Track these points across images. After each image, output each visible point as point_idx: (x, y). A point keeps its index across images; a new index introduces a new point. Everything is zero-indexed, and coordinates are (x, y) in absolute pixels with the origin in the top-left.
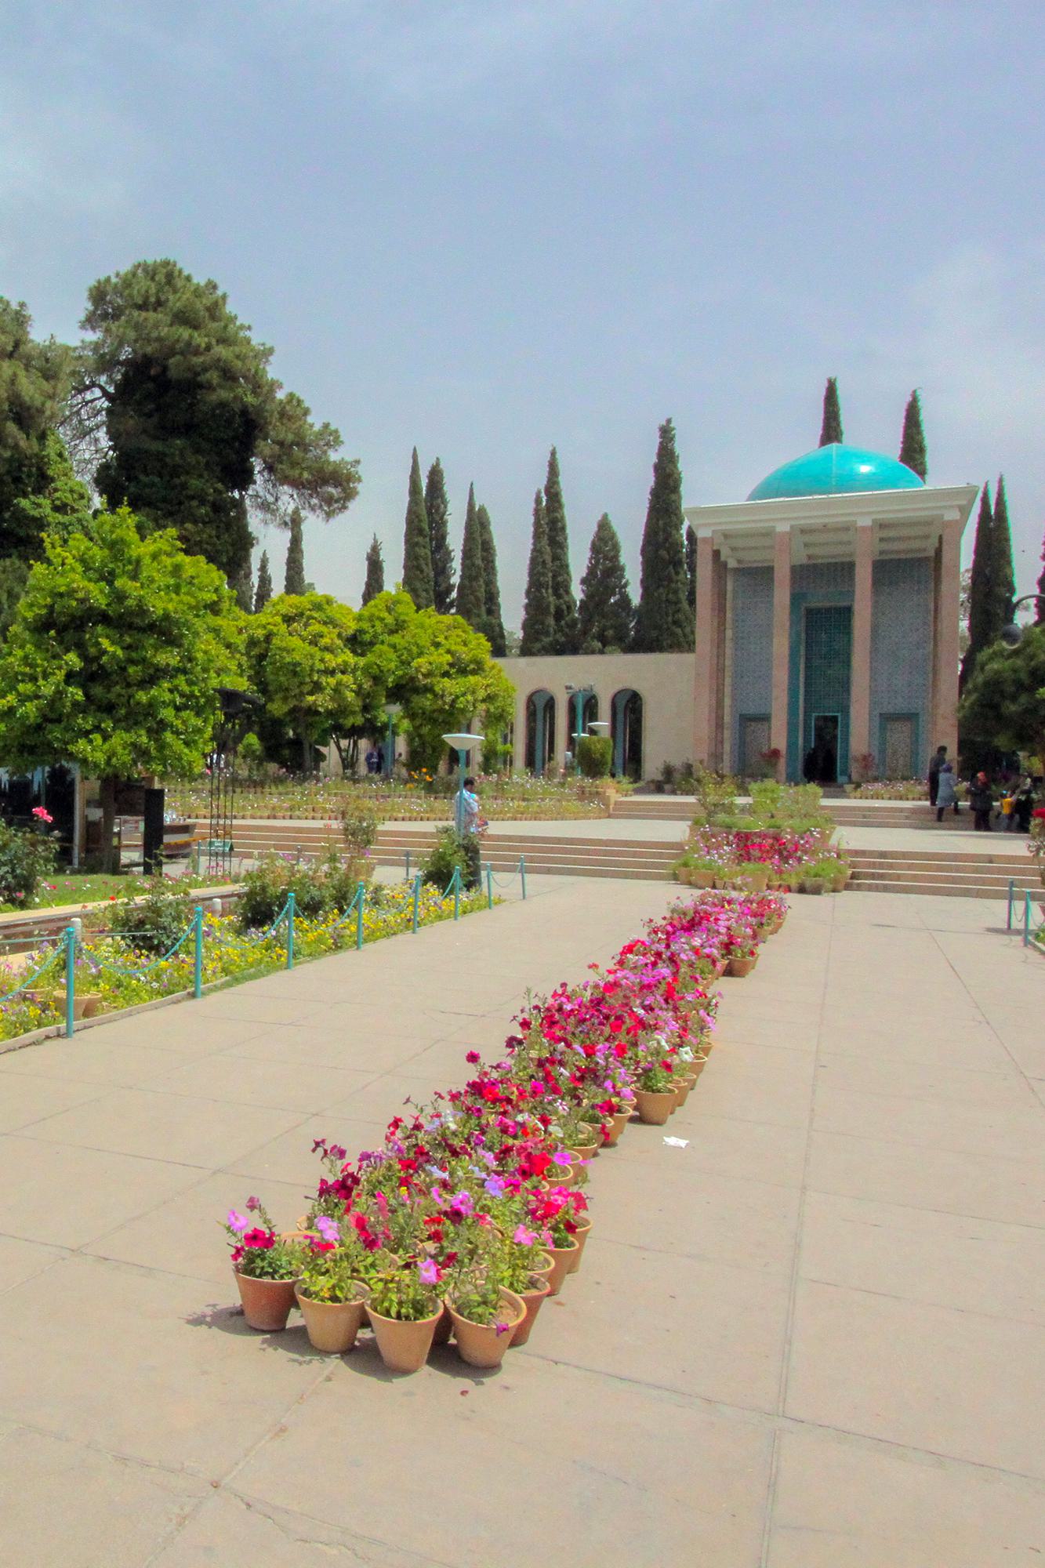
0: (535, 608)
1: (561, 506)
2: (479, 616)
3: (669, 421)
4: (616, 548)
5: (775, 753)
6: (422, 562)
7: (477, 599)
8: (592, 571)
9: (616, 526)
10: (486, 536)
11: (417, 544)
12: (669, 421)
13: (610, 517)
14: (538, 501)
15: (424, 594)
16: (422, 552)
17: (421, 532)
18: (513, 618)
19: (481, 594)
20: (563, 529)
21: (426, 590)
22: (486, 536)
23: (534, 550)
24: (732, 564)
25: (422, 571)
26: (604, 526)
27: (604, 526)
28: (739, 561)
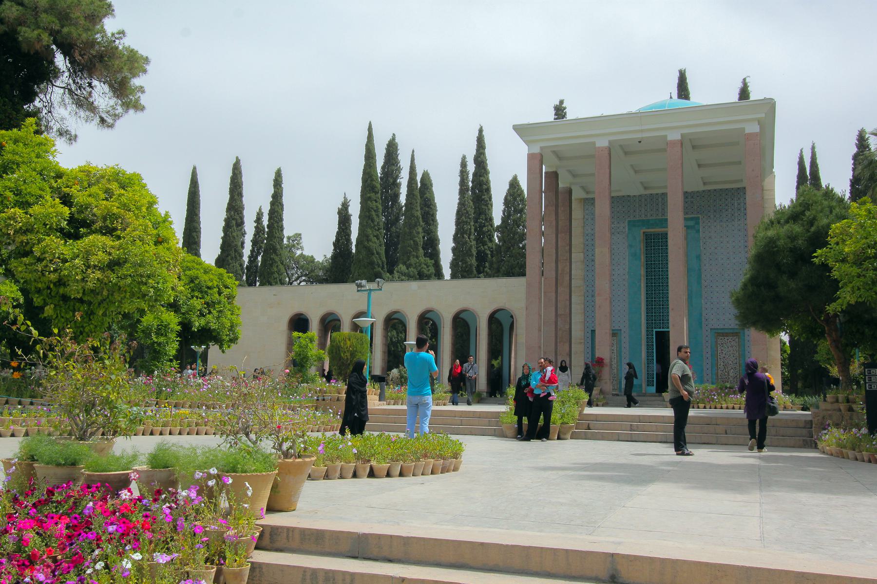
0: (459, 251)
1: (486, 172)
2: (417, 257)
3: (561, 102)
6: (373, 213)
10: (427, 195)
11: (370, 198)
12: (561, 102)
14: (464, 165)
15: (375, 239)
16: (374, 205)
18: (446, 256)
19: (420, 239)
20: (488, 190)
21: (377, 237)
22: (427, 195)
23: (459, 204)
24: (577, 194)
25: (373, 221)
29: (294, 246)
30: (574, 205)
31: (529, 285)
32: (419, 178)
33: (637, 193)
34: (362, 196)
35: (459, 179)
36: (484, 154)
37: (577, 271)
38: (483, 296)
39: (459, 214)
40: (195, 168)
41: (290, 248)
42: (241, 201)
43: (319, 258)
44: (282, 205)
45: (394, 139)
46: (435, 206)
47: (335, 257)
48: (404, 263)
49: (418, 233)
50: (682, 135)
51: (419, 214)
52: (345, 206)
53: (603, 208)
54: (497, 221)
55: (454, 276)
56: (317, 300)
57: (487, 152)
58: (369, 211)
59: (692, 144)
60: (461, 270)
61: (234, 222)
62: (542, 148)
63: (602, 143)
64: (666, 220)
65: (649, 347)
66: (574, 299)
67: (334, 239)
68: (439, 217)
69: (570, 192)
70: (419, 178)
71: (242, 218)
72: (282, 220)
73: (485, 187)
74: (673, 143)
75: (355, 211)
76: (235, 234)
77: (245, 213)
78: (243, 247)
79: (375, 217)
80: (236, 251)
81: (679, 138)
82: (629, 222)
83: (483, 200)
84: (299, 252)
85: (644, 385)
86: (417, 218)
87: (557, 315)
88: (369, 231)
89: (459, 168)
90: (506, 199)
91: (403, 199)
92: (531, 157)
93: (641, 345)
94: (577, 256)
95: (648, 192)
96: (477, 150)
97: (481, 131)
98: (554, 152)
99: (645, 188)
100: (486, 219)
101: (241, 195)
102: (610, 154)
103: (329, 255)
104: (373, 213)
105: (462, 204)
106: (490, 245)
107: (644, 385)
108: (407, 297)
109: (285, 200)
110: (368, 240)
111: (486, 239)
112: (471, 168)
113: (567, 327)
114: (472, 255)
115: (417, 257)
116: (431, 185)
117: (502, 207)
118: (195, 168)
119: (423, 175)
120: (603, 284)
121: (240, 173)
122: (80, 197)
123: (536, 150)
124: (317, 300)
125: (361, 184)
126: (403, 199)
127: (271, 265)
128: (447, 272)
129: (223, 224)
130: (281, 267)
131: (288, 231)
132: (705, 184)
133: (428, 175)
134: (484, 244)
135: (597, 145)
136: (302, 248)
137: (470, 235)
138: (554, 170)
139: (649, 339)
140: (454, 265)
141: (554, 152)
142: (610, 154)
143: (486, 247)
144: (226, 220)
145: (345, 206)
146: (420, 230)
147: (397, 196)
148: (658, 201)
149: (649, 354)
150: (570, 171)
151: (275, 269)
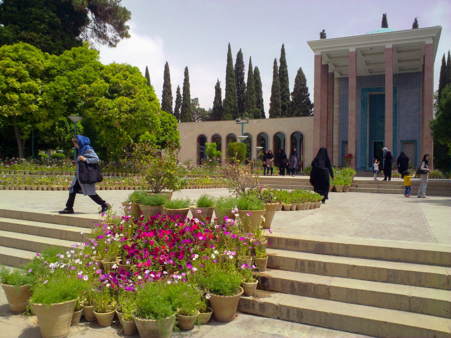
1: (286, 66)
2: (253, 108)
3: (324, 31)
4: (305, 80)
5: (350, 156)
6: (232, 88)
7: (253, 102)
8: (295, 89)
9: (305, 72)
10: (257, 78)
11: (230, 80)
12: (324, 31)
13: (302, 69)
14: (275, 63)
15: (233, 100)
17: (231, 76)
19: (255, 100)
20: (287, 75)
21: (234, 99)
22: (257, 78)
23: (273, 82)
24: (337, 75)
25: (232, 91)
26: (300, 72)
27: (300, 72)
28: (340, 73)
29: (195, 104)
30: (335, 81)
31: (315, 120)
32: (253, 70)
33: (366, 75)
34: (226, 79)
35: (273, 70)
36: (285, 57)
37: (336, 113)
38: (287, 126)
39: (273, 87)
40: (147, 67)
41: (193, 105)
42: (170, 83)
43: (207, 109)
44: (189, 85)
45: (240, 51)
46: (261, 84)
47: (214, 108)
48: (247, 111)
49: (254, 97)
50: (393, 45)
51: (254, 87)
52: (218, 84)
53: (352, 83)
54: (291, 90)
55: (271, 117)
56: (210, 129)
57: (286, 56)
58: (230, 86)
59: (397, 50)
60: (273, 114)
61: (167, 93)
62: (322, 53)
63: (352, 50)
64: (384, 88)
65: (370, 149)
66: (335, 127)
67: (214, 100)
68: (263, 89)
69: (333, 74)
70: (253, 70)
71: (170, 91)
72: (189, 91)
73: (285, 74)
74: (388, 49)
75: (223, 87)
76: (168, 98)
77: (172, 88)
78: (172, 105)
79: (233, 89)
80: (169, 106)
81: (392, 47)
82: (362, 90)
83: (284, 80)
84: (197, 107)
85: (367, 167)
86: (253, 89)
87: (327, 134)
88: (230, 96)
89: (273, 65)
90: (296, 79)
91: (246, 81)
92: (316, 57)
93: (366, 148)
94: (336, 106)
95: (371, 74)
96: (281, 56)
97: (283, 46)
98: (327, 54)
99: (370, 72)
100: (286, 90)
101: (169, 80)
102: (356, 55)
103: (212, 108)
104: (232, 88)
105: (274, 82)
106: (288, 102)
107: (367, 167)
108: (254, 127)
109: (190, 82)
110: (230, 101)
111: (286, 99)
112: (279, 64)
113: (331, 140)
114: (279, 107)
115: (253, 108)
116: (259, 73)
117: (294, 83)
118: (147, 67)
119: (255, 68)
120: (352, 119)
121: (168, 69)
122: (114, 79)
123: (319, 53)
124: (210, 129)
125: (226, 74)
126: (246, 81)
127: (186, 113)
128: (267, 115)
129: (162, 93)
130: (190, 114)
131: (192, 97)
132: (400, 70)
133: (257, 68)
134: (285, 101)
135: (350, 51)
136: (199, 105)
137: (278, 97)
138: (327, 63)
139: (370, 145)
140: (270, 112)
141: (327, 54)
142: (356, 55)
143: (286, 103)
144: (163, 92)
145: (218, 84)
146: (254, 95)
147: (243, 79)
148: (382, 78)
149: (370, 152)
150: (333, 64)
151: (188, 115)
